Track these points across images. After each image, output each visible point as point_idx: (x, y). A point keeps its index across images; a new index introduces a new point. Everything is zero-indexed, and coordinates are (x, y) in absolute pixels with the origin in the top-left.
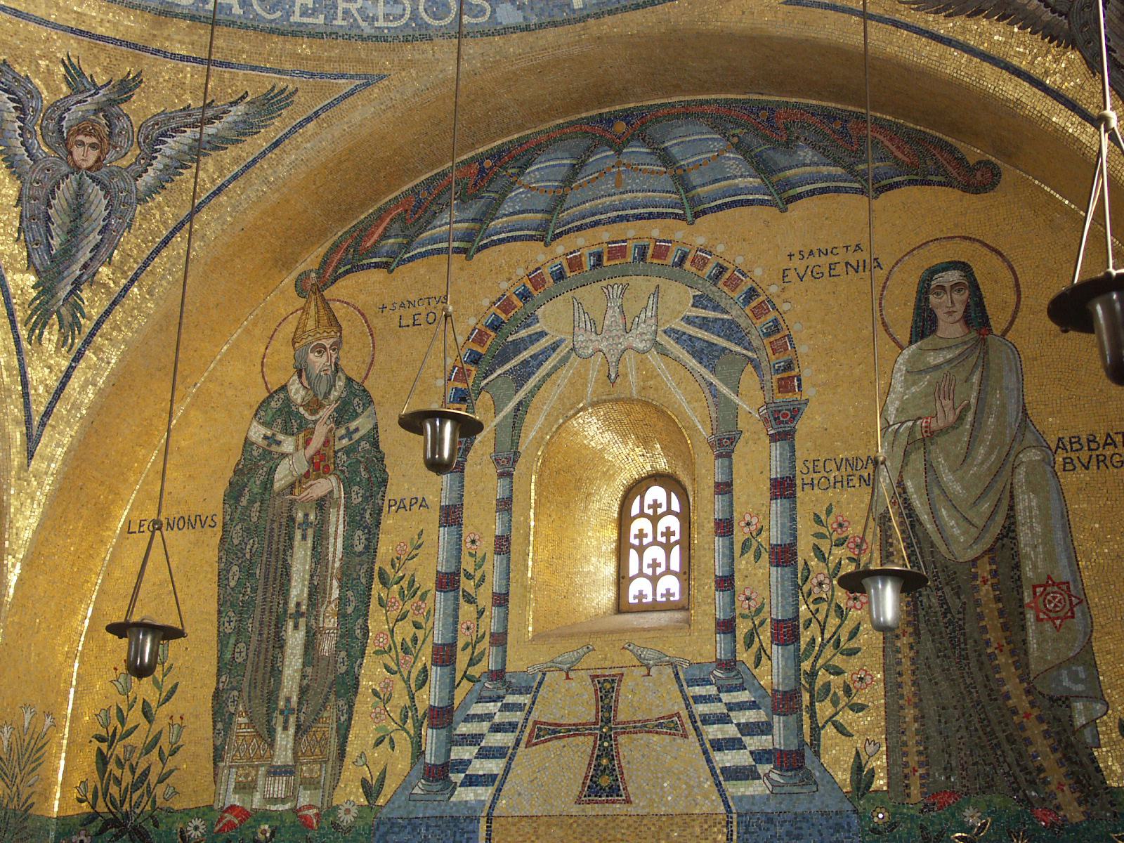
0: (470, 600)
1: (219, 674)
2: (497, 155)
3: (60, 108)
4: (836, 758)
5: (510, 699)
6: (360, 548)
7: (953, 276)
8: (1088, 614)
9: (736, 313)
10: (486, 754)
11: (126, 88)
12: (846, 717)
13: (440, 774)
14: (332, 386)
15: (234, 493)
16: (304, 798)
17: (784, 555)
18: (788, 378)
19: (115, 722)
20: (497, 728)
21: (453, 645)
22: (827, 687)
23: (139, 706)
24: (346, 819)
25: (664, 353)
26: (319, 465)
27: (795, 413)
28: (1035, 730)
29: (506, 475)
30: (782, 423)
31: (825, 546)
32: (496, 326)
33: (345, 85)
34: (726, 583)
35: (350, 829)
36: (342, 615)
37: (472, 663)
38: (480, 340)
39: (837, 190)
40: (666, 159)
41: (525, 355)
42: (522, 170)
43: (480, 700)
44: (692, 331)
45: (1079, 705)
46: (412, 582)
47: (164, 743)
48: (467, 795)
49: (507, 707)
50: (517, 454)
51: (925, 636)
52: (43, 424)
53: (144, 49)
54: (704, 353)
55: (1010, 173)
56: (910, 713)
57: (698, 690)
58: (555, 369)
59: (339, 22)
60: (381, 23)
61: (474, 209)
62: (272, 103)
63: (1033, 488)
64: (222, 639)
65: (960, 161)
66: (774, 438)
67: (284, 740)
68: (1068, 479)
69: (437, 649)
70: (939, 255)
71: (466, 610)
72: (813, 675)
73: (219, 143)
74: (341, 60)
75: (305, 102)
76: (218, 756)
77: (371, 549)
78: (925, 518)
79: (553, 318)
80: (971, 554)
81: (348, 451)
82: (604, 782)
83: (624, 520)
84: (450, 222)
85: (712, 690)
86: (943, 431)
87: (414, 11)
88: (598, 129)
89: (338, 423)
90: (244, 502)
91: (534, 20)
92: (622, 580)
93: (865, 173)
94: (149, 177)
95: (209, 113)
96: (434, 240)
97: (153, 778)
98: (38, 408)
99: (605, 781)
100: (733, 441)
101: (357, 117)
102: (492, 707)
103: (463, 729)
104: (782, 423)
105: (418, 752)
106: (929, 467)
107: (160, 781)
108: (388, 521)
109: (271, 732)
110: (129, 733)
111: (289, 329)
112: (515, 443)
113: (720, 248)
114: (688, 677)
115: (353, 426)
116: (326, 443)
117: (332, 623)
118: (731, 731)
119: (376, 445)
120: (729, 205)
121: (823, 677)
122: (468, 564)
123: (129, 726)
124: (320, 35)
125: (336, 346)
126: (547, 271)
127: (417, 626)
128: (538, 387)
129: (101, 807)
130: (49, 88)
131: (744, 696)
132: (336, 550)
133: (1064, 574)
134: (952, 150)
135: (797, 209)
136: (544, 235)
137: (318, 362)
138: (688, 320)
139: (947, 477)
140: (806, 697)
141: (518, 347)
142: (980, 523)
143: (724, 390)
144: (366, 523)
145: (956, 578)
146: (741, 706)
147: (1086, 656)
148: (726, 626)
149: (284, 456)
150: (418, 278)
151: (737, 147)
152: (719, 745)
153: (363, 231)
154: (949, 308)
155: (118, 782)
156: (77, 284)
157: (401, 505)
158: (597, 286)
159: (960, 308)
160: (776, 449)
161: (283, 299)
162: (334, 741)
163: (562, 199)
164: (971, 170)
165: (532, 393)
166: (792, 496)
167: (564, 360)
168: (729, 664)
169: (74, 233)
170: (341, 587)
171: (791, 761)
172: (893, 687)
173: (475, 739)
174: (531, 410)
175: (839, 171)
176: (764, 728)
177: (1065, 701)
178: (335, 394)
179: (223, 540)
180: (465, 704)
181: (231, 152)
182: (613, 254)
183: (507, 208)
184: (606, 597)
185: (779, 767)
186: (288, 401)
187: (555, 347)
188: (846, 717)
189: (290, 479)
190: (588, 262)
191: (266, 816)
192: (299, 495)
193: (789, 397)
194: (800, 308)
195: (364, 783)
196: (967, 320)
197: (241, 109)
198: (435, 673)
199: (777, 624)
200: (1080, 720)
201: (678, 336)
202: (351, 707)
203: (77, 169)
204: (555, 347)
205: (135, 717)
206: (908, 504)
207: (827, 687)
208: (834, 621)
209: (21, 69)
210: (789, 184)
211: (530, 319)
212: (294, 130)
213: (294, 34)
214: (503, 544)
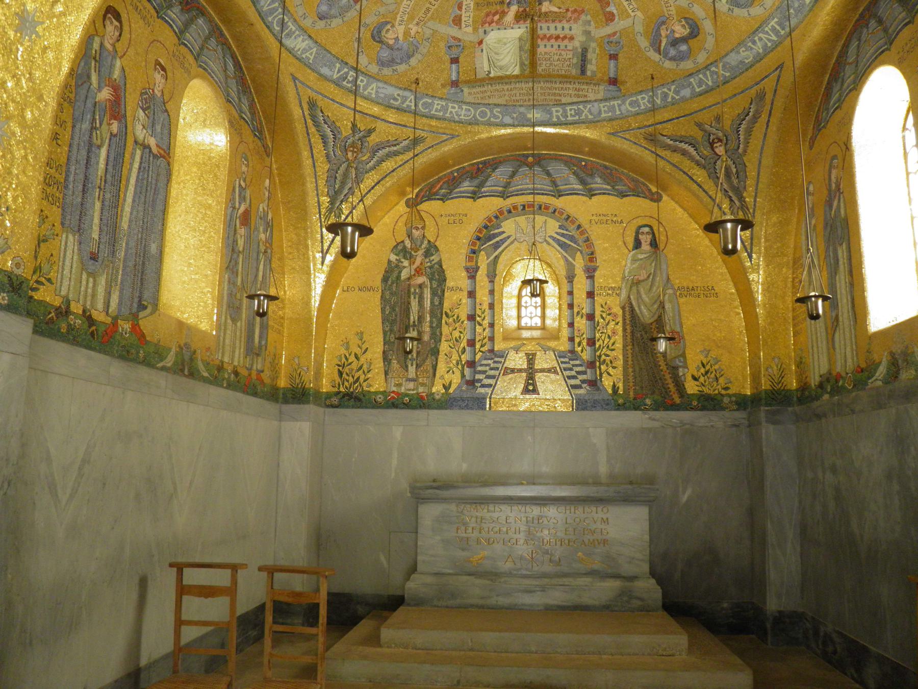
0: (480, 325)
1: (384, 344)
2: (484, 163)
3: (347, 138)
4: (607, 383)
5: (496, 359)
6: (437, 303)
7: (647, 229)
8: (684, 342)
9: (573, 233)
10: (488, 377)
11: (370, 132)
12: (611, 370)
13: (472, 383)
14: (422, 243)
15: (385, 280)
16: (421, 390)
17: (591, 317)
18: (592, 257)
19: (344, 360)
20: (492, 369)
21: (474, 340)
22: (604, 360)
23: (353, 356)
24: (437, 397)
25: (548, 244)
26: (418, 272)
27: (595, 270)
28: (668, 376)
29: (492, 282)
30: (590, 273)
31: (604, 315)
32: (486, 227)
33: (445, 137)
34: (571, 325)
35: (439, 400)
36: (431, 327)
37: (482, 346)
38: (480, 231)
39: (609, 194)
40: (548, 174)
41: (498, 239)
42: (494, 170)
43: (486, 359)
44: (559, 237)
45: (681, 369)
46: (458, 317)
47: (365, 367)
48: (482, 390)
49: (495, 362)
50: (496, 275)
51: (636, 346)
52: (327, 253)
53: (379, 118)
54: (563, 245)
55: (665, 197)
56: (631, 370)
57: (562, 360)
58: (509, 245)
59: (448, 115)
60: (462, 117)
61: (476, 182)
62: (416, 141)
63: (670, 302)
64: (385, 333)
65: (650, 190)
66: (587, 278)
67: (412, 370)
68: (681, 300)
69: (468, 341)
70: (641, 222)
71: (479, 329)
72: (600, 356)
73: (396, 154)
74: (445, 128)
75: (429, 142)
76: (386, 373)
77: (441, 304)
78: (636, 309)
79: (508, 226)
80: (651, 321)
81: (430, 267)
82: (530, 388)
83: (519, 297)
84: (466, 186)
85: (567, 360)
86: (643, 281)
87: (475, 115)
88: (523, 159)
89: (426, 257)
90: (389, 283)
91: (516, 123)
92: (519, 317)
93: (617, 190)
94: (371, 164)
95: (395, 143)
96: (461, 192)
97: (361, 380)
98: (325, 248)
99: (531, 388)
100: (573, 277)
101: (446, 149)
102: (489, 362)
103: (479, 368)
104: (590, 273)
105: (463, 376)
106: (638, 292)
107: (365, 381)
108: (446, 294)
109: (407, 366)
110: (350, 364)
111: (404, 219)
112: (495, 271)
113: (567, 209)
114: (561, 355)
115: (432, 258)
116: (421, 264)
117: (428, 329)
118: (573, 373)
119: (441, 266)
120: (571, 194)
121: (603, 357)
122: (478, 312)
123: (350, 361)
124: (440, 119)
125: (423, 228)
126: (505, 209)
127: (461, 332)
128: (503, 251)
129: (342, 389)
130: (346, 131)
131: (578, 362)
132: (427, 304)
133: (678, 329)
134: (647, 186)
135: (595, 199)
136: (504, 195)
137: (416, 233)
138: (557, 233)
139: (644, 296)
140: (598, 364)
141: (495, 236)
142: (654, 311)
143: (570, 259)
144: (439, 293)
145: (645, 328)
146: (577, 365)
147: (683, 355)
148: (571, 339)
149: (405, 267)
150: (455, 206)
151: (574, 173)
152: (569, 377)
153: (432, 186)
154: (645, 239)
155: (348, 381)
156: (342, 202)
157: (452, 289)
158: (523, 217)
159: (649, 240)
160: (588, 281)
161: (402, 208)
162: (431, 371)
163: (509, 183)
164: (653, 194)
165: (501, 253)
166: (594, 298)
167: (512, 243)
168: (572, 352)
169: (343, 183)
170: (431, 317)
171: (593, 383)
172: (625, 361)
173: (484, 372)
174: (501, 259)
175: (609, 187)
176: (584, 373)
177: (676, 368)
178: (423, 246)
179: (382, 297)
180: (480, 360)
181: (401, 157)
182: (529, 206)
183: (488, 184)
184: (513, 323)
185: (589, 385)
186: (405, 247)
187: (509, 237)
188: (611, 370)
189: (408, 276)
190: (520, 208)
191: (407, 395)
192: (412, 282)
193: (593, 264)
194: (596, 233)
195: (444, 385)
196: (651, 244)
197: (407, 141)
198: (468, 349)
199: (589, 340)
200: (681, 374)
201: (554, 239)
202: (437, 359)
203: (348, 160)
204: (509, 237)
205: (352, 358)
206: (631, 304)
207: (604, 360)
208: (607, 340)
209: (338, 124)
210: (591, 190)
211: (499, 226)
212: (423, 151)
213: (431, 118)
214: (491, 306)
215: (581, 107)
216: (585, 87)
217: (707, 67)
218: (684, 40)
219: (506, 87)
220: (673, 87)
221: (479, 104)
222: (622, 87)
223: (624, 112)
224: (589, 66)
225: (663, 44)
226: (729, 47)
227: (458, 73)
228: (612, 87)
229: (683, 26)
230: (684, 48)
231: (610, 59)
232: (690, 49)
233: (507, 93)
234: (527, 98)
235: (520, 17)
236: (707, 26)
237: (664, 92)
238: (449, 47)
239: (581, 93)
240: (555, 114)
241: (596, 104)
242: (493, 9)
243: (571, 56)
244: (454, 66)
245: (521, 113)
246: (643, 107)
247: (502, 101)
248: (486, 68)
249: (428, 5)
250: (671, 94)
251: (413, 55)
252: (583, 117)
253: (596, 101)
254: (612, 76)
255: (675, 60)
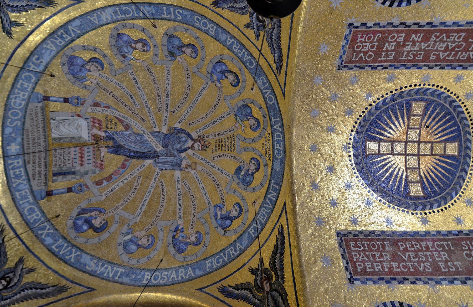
87: (13, 108)
215: (24, 177)
216: (43, 177)
217: (73, 246)
218: (91, 226)
219: (41, 130)
220: (52, 231)
221: (26, 112)
222: (46, 199)
223: (23, 206)
224: (61, 177)
225: (85, 215)
226: (93, 253)
227: (56, 101)
228: (44, 194)
229: (101, 223)
230: (85, 227)
231: (68, 188)
232: (86, 231)
233: (35, 130)
234: (31, 142)
235: (97, 139)
236: (105, 235)
237: (46, 227)
238: (78, 99)
239: (37, 175)
240: (16, 161)
241: (28, 186)
242: (104, 125)
243: (68, 165)
244: (62, 100)
245: (15, 139)
246: (29, 217)
247: (27, 125)
248: (57, 118)
249: (110, 92)
250: (45, 232)
251: (74, 77)
252: (13, 180)
253: (31, 186)
254: (54, 192)
255: (74, 225)
